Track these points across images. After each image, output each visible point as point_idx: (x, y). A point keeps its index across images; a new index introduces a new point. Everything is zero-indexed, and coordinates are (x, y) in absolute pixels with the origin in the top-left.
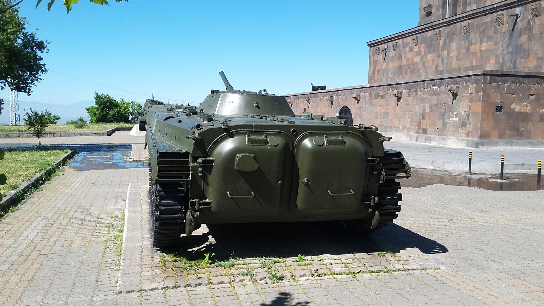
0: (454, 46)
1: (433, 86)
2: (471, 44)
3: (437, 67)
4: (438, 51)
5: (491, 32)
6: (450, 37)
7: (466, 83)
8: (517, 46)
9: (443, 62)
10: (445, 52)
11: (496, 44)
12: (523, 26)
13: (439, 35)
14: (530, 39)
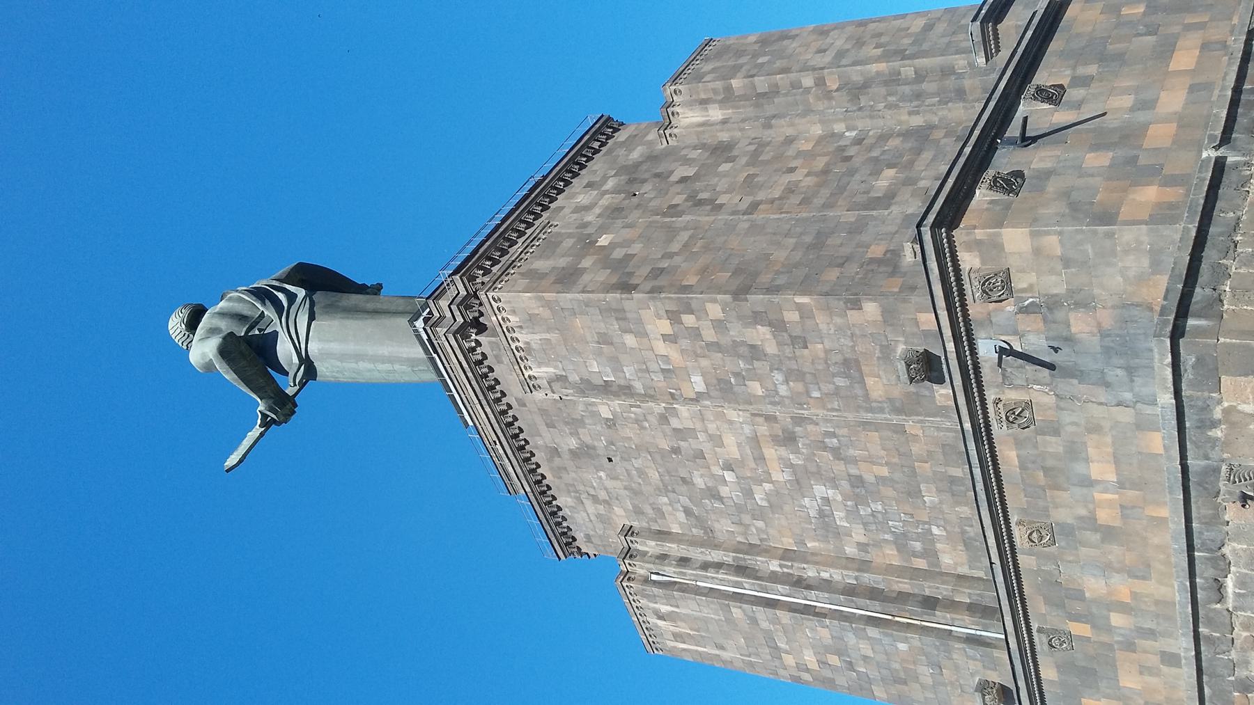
0: (1094, 585)
1: (1221, 598)
2: (1090, 522)
4: (1110, 647)
5: (1054, 445)
6: (1066, 597)
7: (1214, 424)
8: (1107, 351)
9: (1151, 634)
10: (1117, 619)
11: (1095, 429)
12: (1038, 332)
13: (1058, 639)
14: (1084, 303)
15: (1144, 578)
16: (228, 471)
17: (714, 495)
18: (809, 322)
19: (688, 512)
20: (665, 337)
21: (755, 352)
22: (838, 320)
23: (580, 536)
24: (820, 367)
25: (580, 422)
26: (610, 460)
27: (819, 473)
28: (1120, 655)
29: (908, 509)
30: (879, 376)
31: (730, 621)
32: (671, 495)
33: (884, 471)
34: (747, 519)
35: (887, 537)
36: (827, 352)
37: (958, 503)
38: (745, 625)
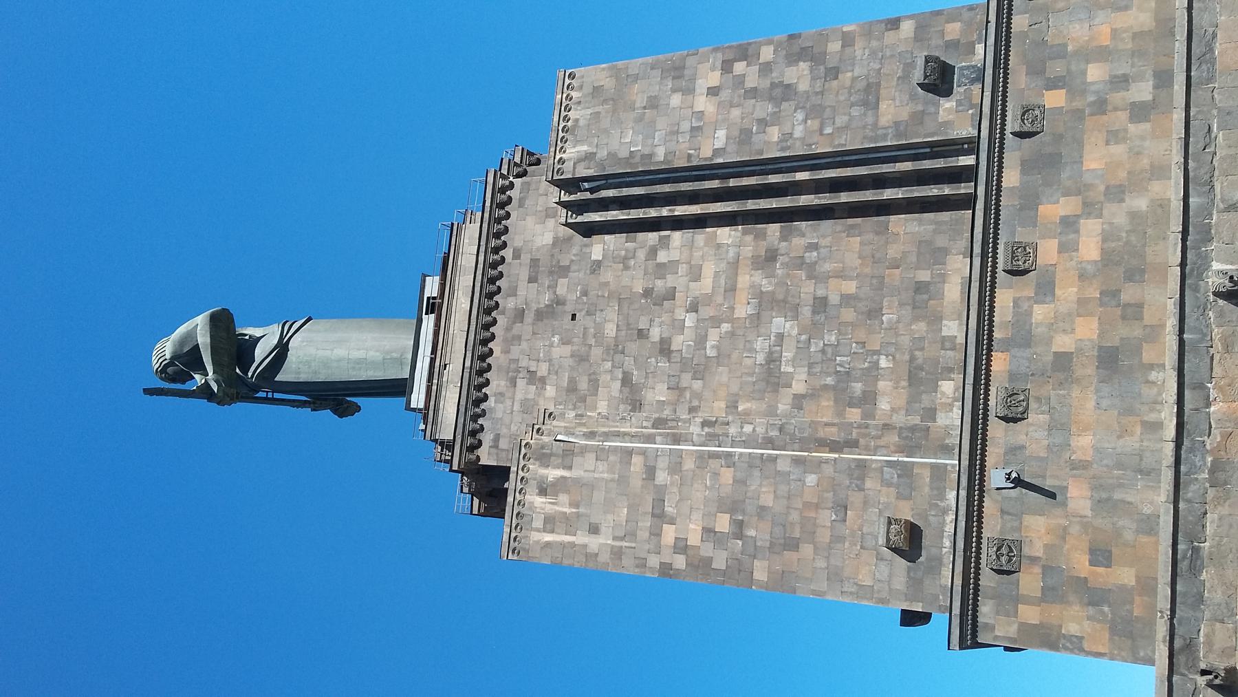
0: (1075, 31)
3: (1139, 112)
4: (1078, 115)
6: (1046, 55)
10: (1095, 73)
15: (1126, 8)
17: (664, 348)
18: (848, 50)
19: (626, 380)
20: (713, 92)
21: (784, 92)
22: (874, 43)
23: (487, 438)
24: (842, 98)
25: (564, 271)
26: (574, 317)
27: (785, 301)
28: (1089, 122)
29: (861, 335)
30: (894, 99)
31: (623, 480)
32: (618, 357)
33: (850, 287)
34: (686, 380)
35: (830, 381)
36: (854, 79)
37: (916, 319)
38: (636, 483)
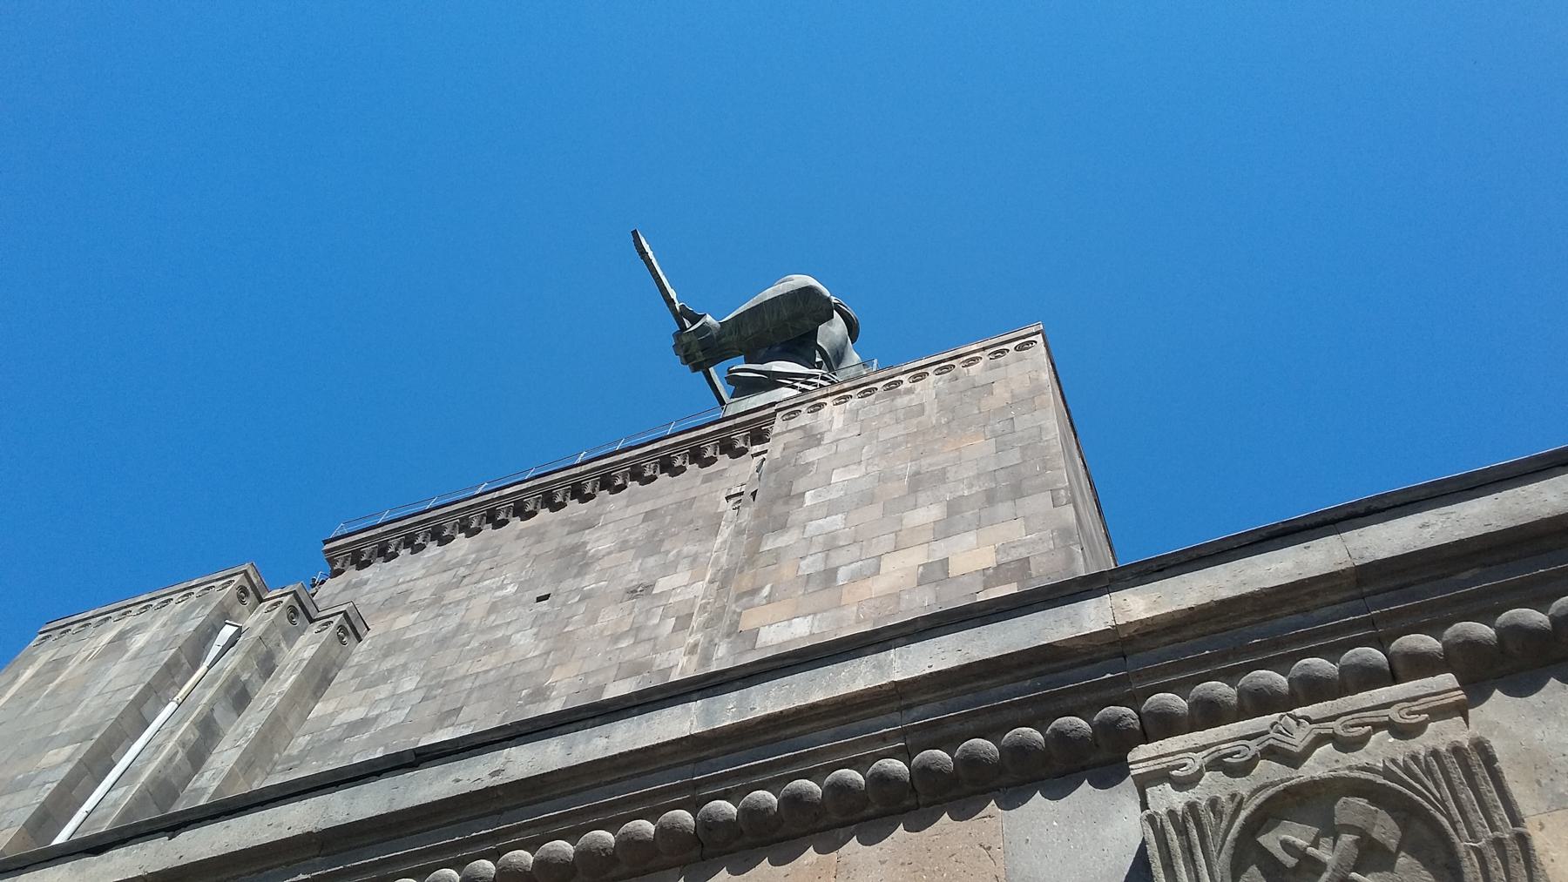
16: (635, 233)
